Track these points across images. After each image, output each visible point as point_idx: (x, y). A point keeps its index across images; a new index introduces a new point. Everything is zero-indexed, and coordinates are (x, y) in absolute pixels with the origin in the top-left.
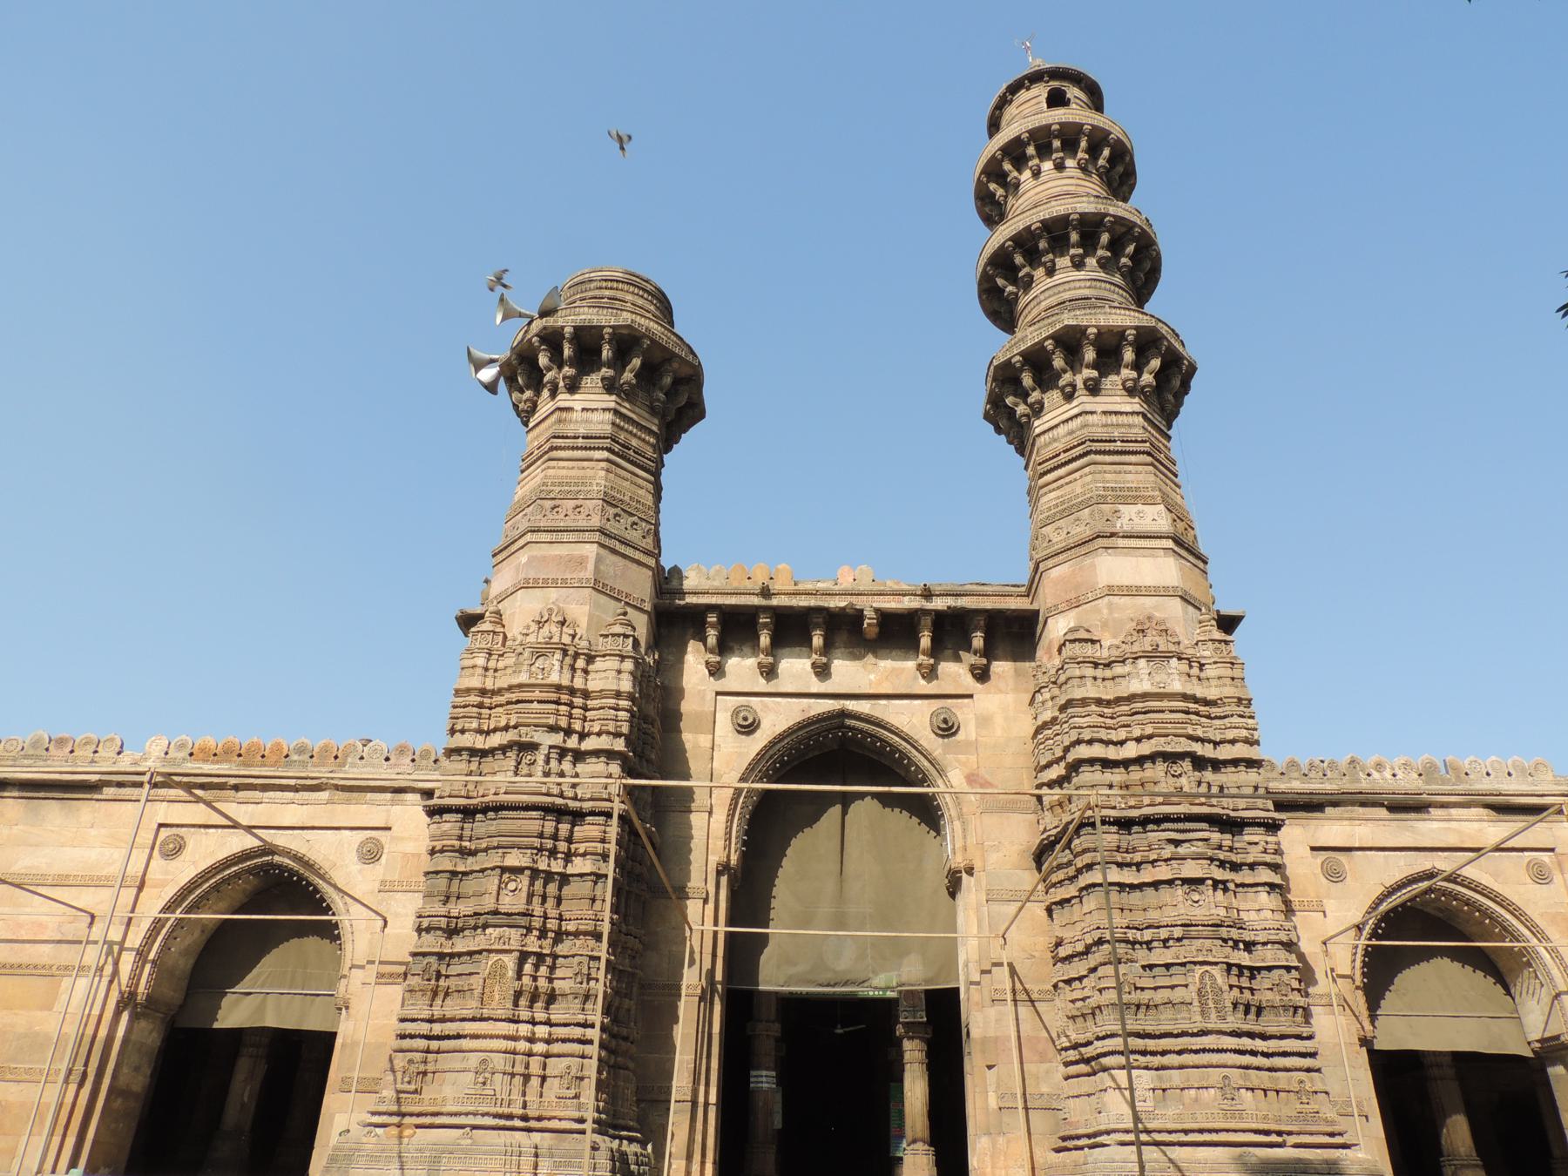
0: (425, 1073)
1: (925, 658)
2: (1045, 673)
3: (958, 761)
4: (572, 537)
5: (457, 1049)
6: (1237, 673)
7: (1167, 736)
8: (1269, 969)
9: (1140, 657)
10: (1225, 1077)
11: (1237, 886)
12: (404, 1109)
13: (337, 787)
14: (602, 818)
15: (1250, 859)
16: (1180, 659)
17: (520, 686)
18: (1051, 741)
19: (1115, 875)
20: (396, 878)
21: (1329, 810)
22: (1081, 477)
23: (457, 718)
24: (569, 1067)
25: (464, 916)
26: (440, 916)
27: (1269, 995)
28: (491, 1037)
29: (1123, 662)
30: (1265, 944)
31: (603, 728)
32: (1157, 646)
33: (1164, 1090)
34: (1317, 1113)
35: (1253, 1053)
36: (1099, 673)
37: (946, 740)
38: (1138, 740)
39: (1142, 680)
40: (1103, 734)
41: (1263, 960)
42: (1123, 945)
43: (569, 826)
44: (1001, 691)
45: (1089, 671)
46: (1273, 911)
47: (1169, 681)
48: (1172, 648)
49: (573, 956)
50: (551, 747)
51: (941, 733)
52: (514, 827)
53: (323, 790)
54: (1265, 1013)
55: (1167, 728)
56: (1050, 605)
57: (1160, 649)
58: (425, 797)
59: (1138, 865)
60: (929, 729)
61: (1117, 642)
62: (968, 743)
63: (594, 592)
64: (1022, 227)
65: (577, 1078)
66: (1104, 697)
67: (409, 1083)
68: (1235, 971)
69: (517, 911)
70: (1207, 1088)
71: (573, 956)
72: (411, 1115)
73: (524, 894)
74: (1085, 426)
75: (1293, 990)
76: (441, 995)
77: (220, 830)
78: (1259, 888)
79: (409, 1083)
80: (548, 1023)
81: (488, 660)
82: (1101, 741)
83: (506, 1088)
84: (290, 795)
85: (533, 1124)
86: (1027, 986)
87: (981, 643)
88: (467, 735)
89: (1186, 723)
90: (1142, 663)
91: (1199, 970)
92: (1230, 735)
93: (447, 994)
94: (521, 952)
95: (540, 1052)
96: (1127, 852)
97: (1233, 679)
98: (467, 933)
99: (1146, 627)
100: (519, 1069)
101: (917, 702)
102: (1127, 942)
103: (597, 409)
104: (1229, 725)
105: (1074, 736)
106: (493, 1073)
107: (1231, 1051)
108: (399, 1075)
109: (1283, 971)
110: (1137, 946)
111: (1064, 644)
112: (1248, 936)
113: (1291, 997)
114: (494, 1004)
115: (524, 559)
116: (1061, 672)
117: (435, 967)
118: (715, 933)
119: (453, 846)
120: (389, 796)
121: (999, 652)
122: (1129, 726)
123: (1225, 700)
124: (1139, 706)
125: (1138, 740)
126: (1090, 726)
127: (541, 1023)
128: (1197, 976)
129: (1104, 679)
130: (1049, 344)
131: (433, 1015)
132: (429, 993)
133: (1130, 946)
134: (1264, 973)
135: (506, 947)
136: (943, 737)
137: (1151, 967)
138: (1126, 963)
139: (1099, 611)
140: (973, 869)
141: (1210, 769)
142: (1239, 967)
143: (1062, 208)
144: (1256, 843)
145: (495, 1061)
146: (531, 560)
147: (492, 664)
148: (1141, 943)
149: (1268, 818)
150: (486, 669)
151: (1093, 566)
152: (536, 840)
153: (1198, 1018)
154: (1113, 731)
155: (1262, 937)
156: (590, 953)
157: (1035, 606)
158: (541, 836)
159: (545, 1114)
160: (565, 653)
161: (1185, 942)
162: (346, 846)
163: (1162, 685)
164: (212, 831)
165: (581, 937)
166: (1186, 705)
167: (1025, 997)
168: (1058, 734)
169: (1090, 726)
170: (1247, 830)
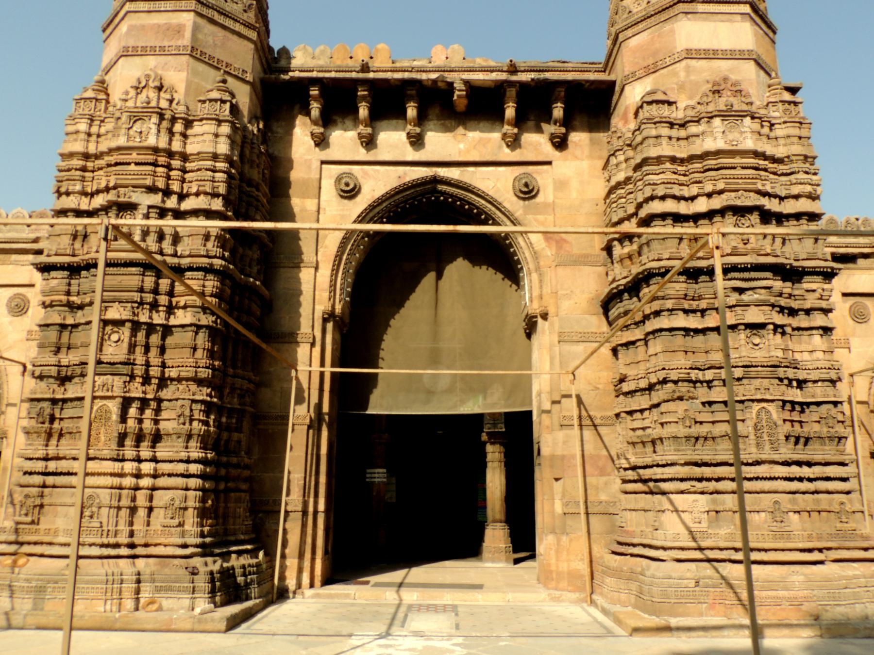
0: (42, 506)
1: (510, 128)
2: (620, 137)
3: (536, 220)
5: (68, 485)
6: (804, 133)
7: (738, 191)
8: (818, 404)
9: (716, 116)
10: (776, 502)
11: (794, 329)
12: (21, 539)
14: (200, 273)
15: (808, 305)
16: (753, 118)
17: (119, 149)
18: (623, 200)
19: (681, 321)
21: (861, 262)
23: (61, 181)
24: (173, 499)
25: (74, 365)
26: (51, 365)
27: (816, 427)
28: (99, 474)
29: (698, 121)
30: (815, 382)
31: (201, 188)
32: (732, 106)
33: (717, 512)
34: (854, 530)
35: (800, 479)
36: (674, 133)
37: (527, 202)
38: (709, 195)
39: (715, 139)
40: (676, 191)
41: (813, 396)
42: (686, 384)
43: (153, 279)
44: (576, 158)
45: (665, 131)
46: (824, 352)
47: (741, 139)
48: (745, 107)
49: (177, 400)
50: (149, 207)
51: (522, 196)
52: (114, 283)
54: (811, 442)
55: (738, 184)
56: (627, 73)
57: (734, 109)
59: (703, 312)
60: (512, 193)
61: (692, 103)
62: (546, 205)
63: (192, 60)
65: (180, 508)
66: (679, 155)
67: (26, 515)
68: (788, 406)
69: (118, 361)
70: (758, 512)
71: (177, 400)
72: (29, 543)
73: (125, 345)
75: (839, 422)
76: (56, 436)
78: (814, 332)
79: (26, 515)
80: (154, 460)
81: (91, 126)
82: (674, 197)
83: (113, 521)
85: (139, 551)
86: (591, 413)
87: (561, 113)
88: (72, 197)
89: (756, 178)
90: (717, 121)
91: (756, 407)
92: (796, 190)
93: (61, 435)
94: (124, 398)
95: (146, 486)
96: (693, 300)
97: (800, 138)
98: (76, 380)
99: (721, 88)
100: (125, 502)
101: (502, 169)
102: (690, 381)
104: (795, 181)
105: (648, 192)
106: (100, 508)
107: (781, 479)
108: (18, 507)
109: (831, 406)
110: (698, 385)
111: (641, 107)
112: (802, 375)
113: (837, 429)
114: (101, 445)
116: (638, 132)
117: (48, 411)
118: (322, 374)
119: (61, 301)
121: (576, 123)
122: (700, 182)
123: (794, 158)
124: (711, 163)
125: (709, 195)
126: (664, 183)
127: (146, 460)
128: (754, 412)
129: (678, 139)
131: (47, 454)
132: (43, 435)
133: (691, 385)
134: (813, 408)
135: (110, 394)
136: (524, 199)
137: (710, 403)
138: (687, 400)
139: (675, 74)
140: (547, 314)
141: (774, 222)
142: (793, 403)
144: (814, 291)
145: (102, 496)
146: (131, 28)
147: (94, 129)
148: (701, 382)
149: (827, 268)
150: (89, 135)
151: (672, 31)
152: (135, 294)
153: (754, 450)
154: (685, 188)
155: (814, 376)
156: (192, 397)
157: (612, 77)
158: (141, 290)
159: (150, 541)
160: (162, 117)
161: (745, 381)
163: (735, 143)
165: (184, 382)
166: (757, 161)
167: (589, 422)
168: (632, 193)
169: (664, 183)
170: (807, 278)
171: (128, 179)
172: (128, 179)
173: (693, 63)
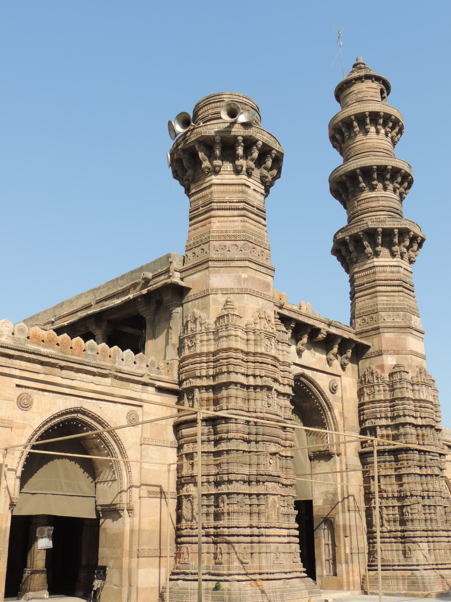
4: (264, 270)
6: (436, 394)
13: (116, 377)
20: (149, 437)
22: (398, 296)
28: (274, 536)
52: (270, 431)
53: (108, 377)
58: (157, 391)
64: (384, 164)
74: (398, 272)
77: (51, 394)
84: (90, 377)
101: (325, 375)
103: (258, 192)
115: (244, 276)
120: (140, 386)
124: (423, 404)
130: (396, 231)
143: (401, 165)
162: (120, 413)
164: (46, 393)
171: (269, 373)
172: (269, 373)
173: (413, 356)
